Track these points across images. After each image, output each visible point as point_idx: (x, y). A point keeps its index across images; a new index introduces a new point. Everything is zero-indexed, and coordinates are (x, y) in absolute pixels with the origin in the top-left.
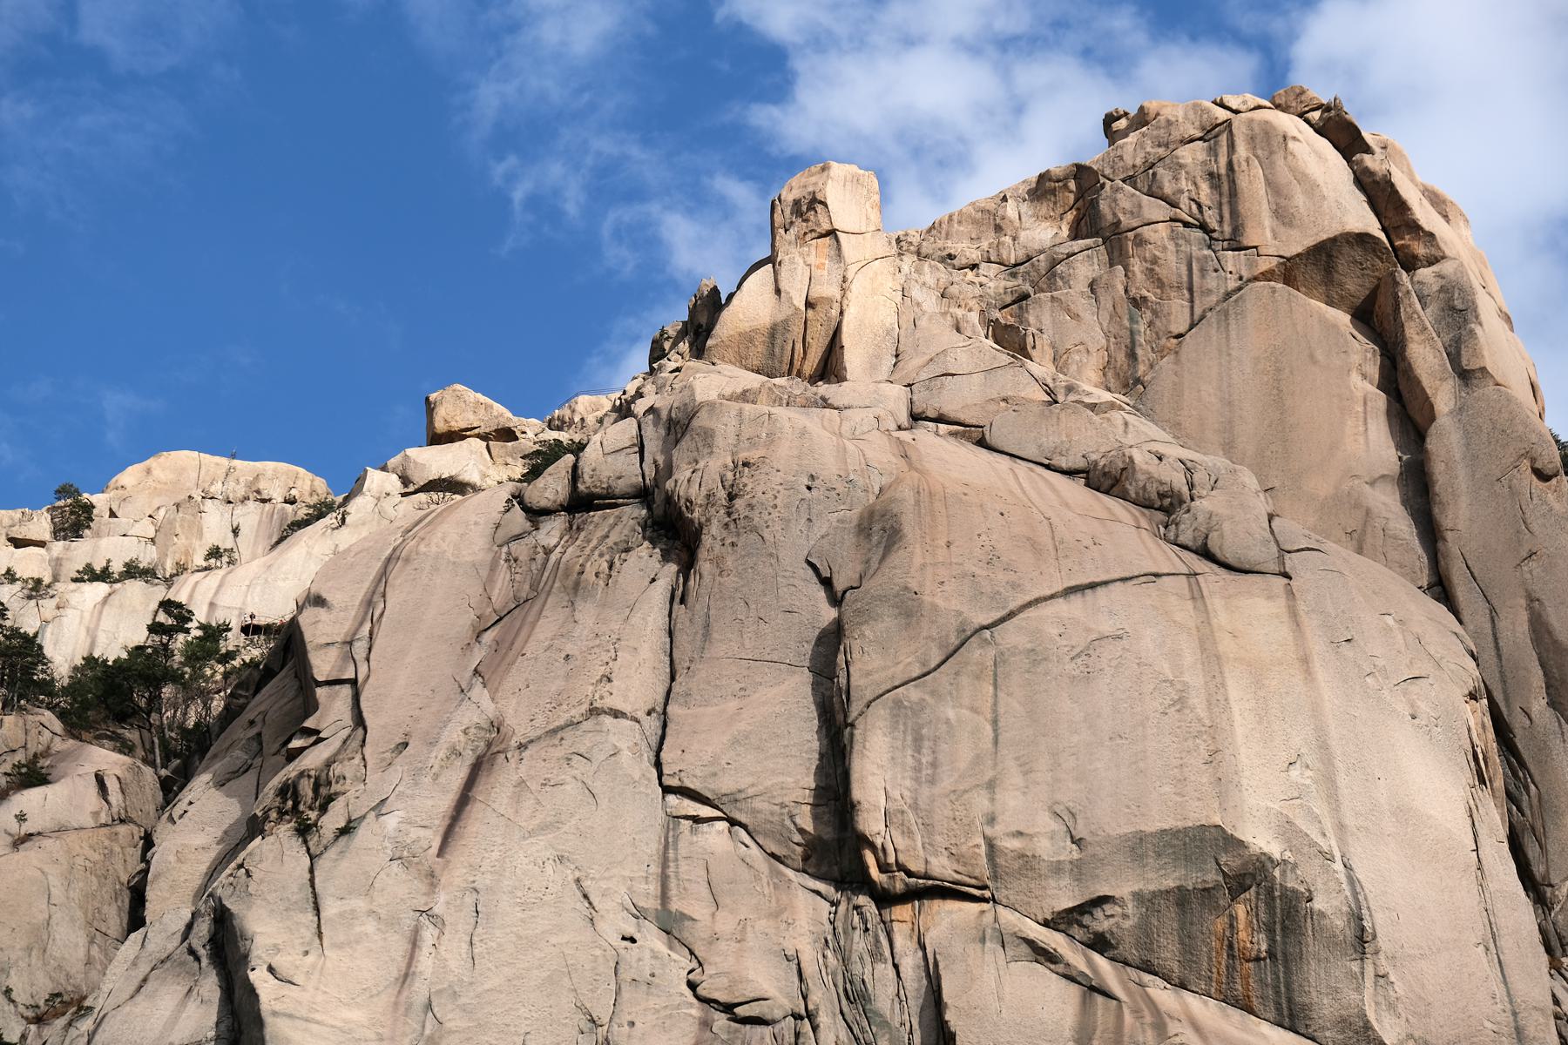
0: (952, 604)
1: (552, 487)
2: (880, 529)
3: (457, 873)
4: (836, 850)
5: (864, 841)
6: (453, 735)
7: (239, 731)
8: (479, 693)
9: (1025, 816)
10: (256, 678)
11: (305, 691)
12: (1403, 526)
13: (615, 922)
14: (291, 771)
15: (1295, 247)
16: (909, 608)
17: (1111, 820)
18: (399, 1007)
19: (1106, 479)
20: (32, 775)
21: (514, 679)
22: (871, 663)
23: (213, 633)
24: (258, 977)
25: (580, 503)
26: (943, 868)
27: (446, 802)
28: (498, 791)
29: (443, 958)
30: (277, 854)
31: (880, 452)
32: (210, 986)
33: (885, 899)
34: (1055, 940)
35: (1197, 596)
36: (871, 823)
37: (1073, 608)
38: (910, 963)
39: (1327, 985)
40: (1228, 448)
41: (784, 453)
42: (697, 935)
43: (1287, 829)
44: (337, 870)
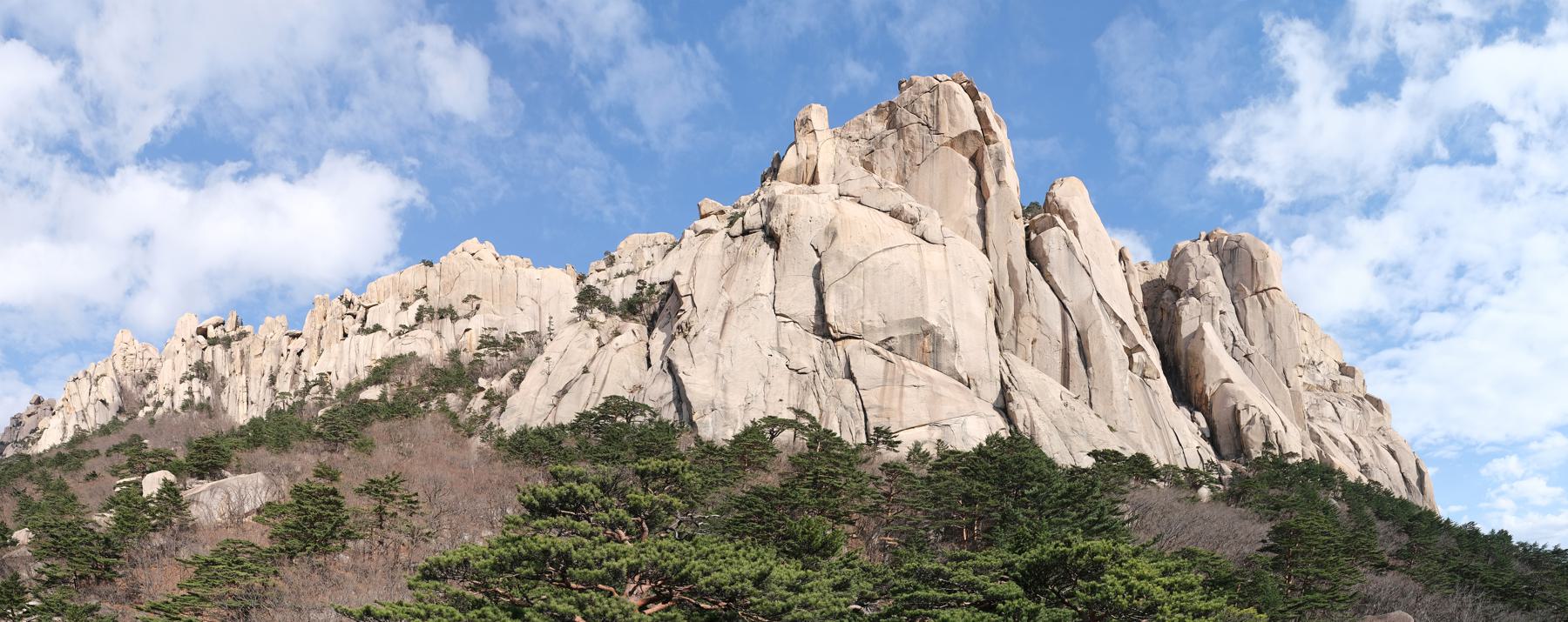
0: (852, 255)
1: (737, 229)
3: (725, 343)
4: (822, 328)
6: (719, 306)
7: (664, 312)
9: (871, 316)
10: (667, 296)
11: (679, 297)
13: (766, 351)
16: (840, 257)
17: (894, 317)
20: (617, 334)
21: (733, 288)
22: (828, 275)
26: (850, 331)
28: (732, 320)
29: (725, 365)
30: (679, 342)
31: (831, 208)
32: (670, 378)
33: (835, 340)
34: (878, 349)
36: (831, 320)
38: (842, 356)
39: (945, 358)
41: (802, 211)
42: (788, 352)
43: (940, 319)
44: (695, 346)
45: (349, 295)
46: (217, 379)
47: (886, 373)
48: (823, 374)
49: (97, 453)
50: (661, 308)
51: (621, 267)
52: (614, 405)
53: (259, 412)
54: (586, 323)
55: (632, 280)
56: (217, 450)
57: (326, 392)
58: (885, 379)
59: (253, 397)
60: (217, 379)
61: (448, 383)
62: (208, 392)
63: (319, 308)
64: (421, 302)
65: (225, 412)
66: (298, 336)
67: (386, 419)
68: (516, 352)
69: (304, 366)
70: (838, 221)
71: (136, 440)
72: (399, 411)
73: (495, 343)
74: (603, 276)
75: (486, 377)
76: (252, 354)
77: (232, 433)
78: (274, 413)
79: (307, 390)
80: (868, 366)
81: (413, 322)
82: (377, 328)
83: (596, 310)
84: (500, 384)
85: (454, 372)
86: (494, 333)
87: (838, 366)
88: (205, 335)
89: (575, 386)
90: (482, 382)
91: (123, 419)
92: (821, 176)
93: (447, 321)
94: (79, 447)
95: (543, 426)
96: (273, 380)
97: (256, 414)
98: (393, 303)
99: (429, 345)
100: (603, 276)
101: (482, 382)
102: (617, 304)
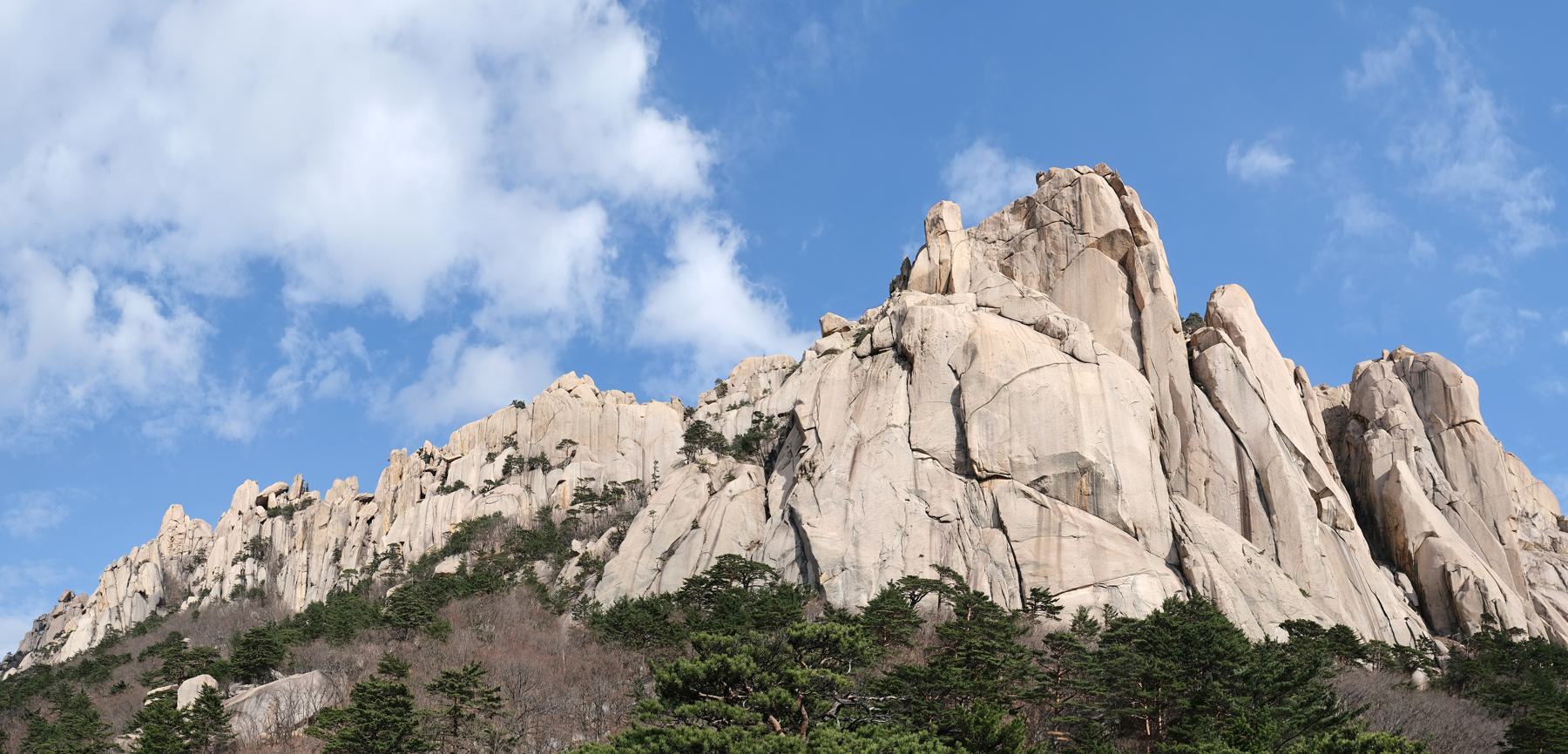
0: (995, 377)
1: (865, 348)
2: (971, 352)
3: (855, 485)
4: (965, 466)
5: (973, 461)
6: (848, 441)
7: (784, 451)
8: (853, 425)
9: (1020, 451)
10: (786, 431)
11: (801, 431)
12: (1133, 347)
13: (903, 495)
14: (802, 461)
15: (1101, 235)
16: (982, 380)
17: (1046, 451)
18: (846, 529)
19: (1041, 327)
20: (731, 478)
21: (863, 418)
22: (970, 400)
23: (770, 419)
24: (805, 526)
25: (875, 352)
26: (997, 469)
27: (849, 463)
28: (863, 457)
29: (855, 513)
30: (803, 487)
32: (792, 532)
33: (980, 480)
35: (1070, 371)
36: (975, 456)
37: (1032, 376)
39: (1107, 502)
40: (1080, 315)
41: (937, 325)
42: (927, 496)
43: (1098, 453)
44: (821, 490)
45: (429, 447)
46: (275, 558)
47: (1040, 521)
48: (968, 522)
49: (128, 658)
50: (781, 445)
51: (734, 397)
52: (729, 567)
53: (319, 595)
54: (695, 467)
55: (747, 412)
56: (269, 645)
57: (397, 566)
58: (1040, 529)
59: (314, 579)
60: (275, 558)
61: (536, 548)
62: (263, 574)
63: (395, 466)
64: (510, 451)
65: (280, 597)
66: (369, 500)
67: (465, 596)
68: (614, 505)
69: (374, 536)
70: (977, 336)
71: (176, 637)
72: (480, 585)
73: (592, 497)
74: (713, 408)
75: (581, 538)
76: (316, 526)
77: (287, 623)
78: (337, 595)
79: (375, 565)
80: (1019, 512)
81: (500, 475)
82: (459, 485)
83: (706, 450)
84: (597, 547)
85: (544, 534)
86: (591, 485)
87: (986, 513)
88: (265, 506)
89: (684, 545)
90: (576, 545)
91: (162, 613)
92: (956, 283)
93: (539, 472)
94: (108, 652)
95: (647, 596)
96: (338, 555)
97: (316, 599)
98: (478, 454)
99: (516, 504)
100: (713, 408)
101: (576, 545)
102: (730, 442)
